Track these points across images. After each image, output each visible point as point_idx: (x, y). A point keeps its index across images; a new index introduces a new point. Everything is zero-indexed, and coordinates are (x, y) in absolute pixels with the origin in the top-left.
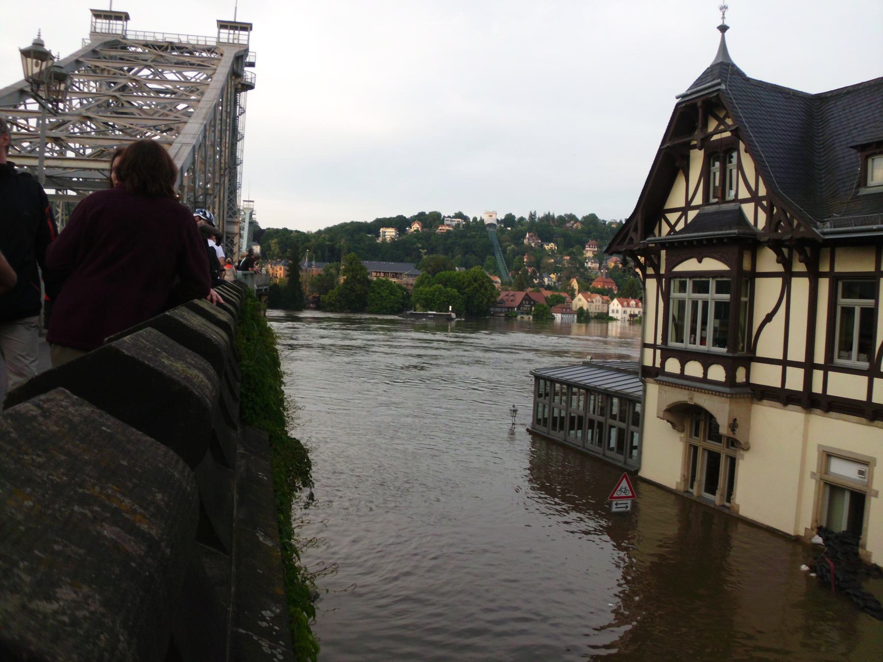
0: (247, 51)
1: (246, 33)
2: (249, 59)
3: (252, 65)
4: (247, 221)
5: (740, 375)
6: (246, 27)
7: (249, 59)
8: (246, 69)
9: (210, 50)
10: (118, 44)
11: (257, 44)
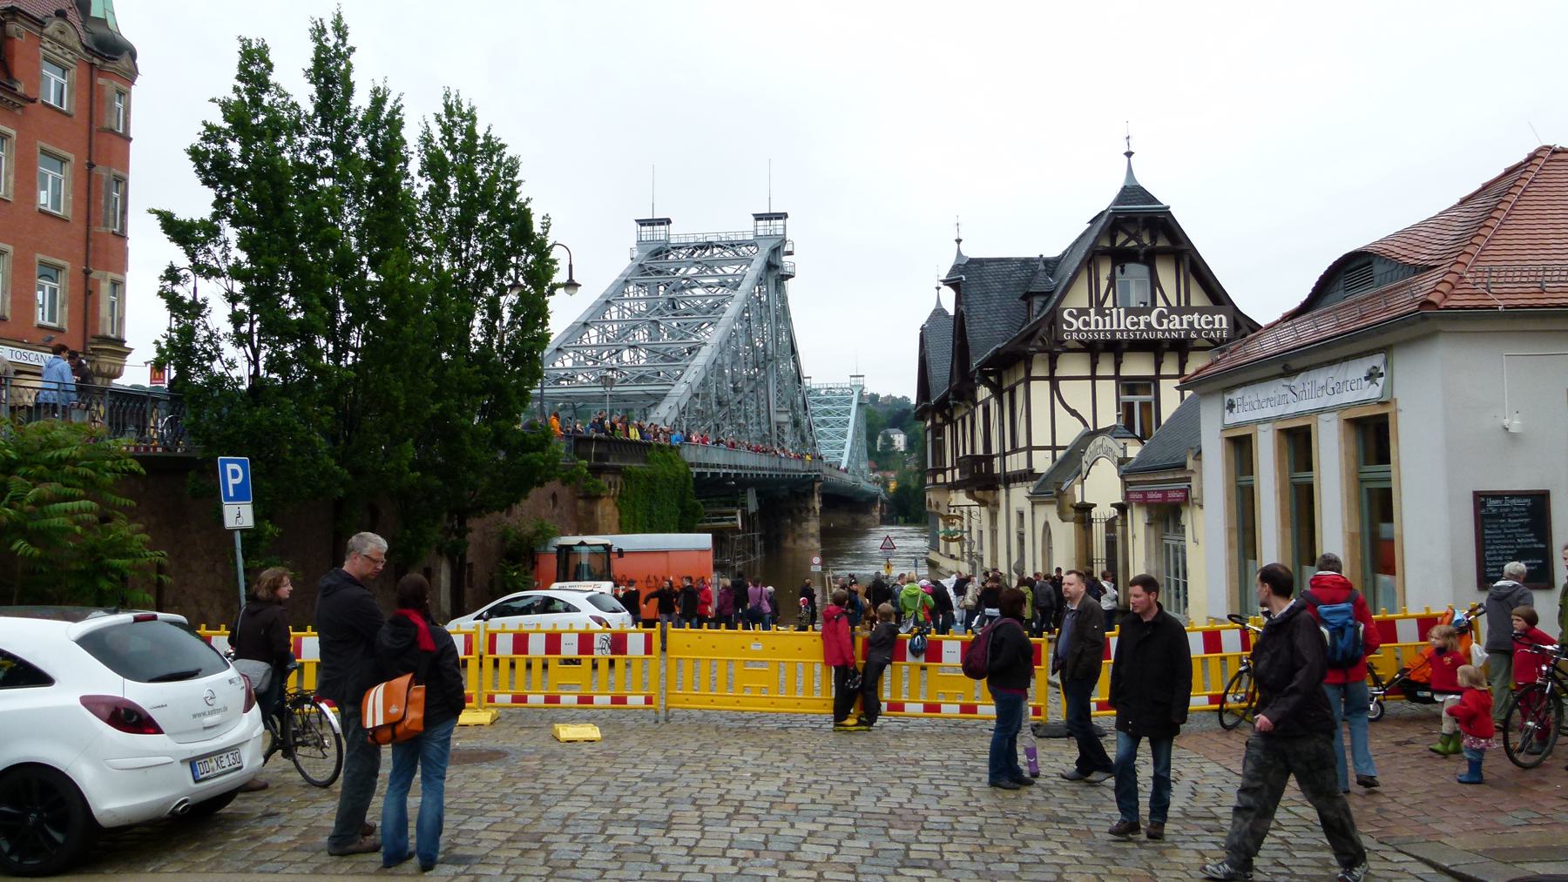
0: (784, 241)
1: (780, 222)
2: (788, 248)
3: (790, 253)
4: (855, 402)
5: (940, 478)
6: (782, 216)
7: (788, 248)
8: (785, 258)
9: (748, 244)
10: (661, 252)
11: (794, 231)
